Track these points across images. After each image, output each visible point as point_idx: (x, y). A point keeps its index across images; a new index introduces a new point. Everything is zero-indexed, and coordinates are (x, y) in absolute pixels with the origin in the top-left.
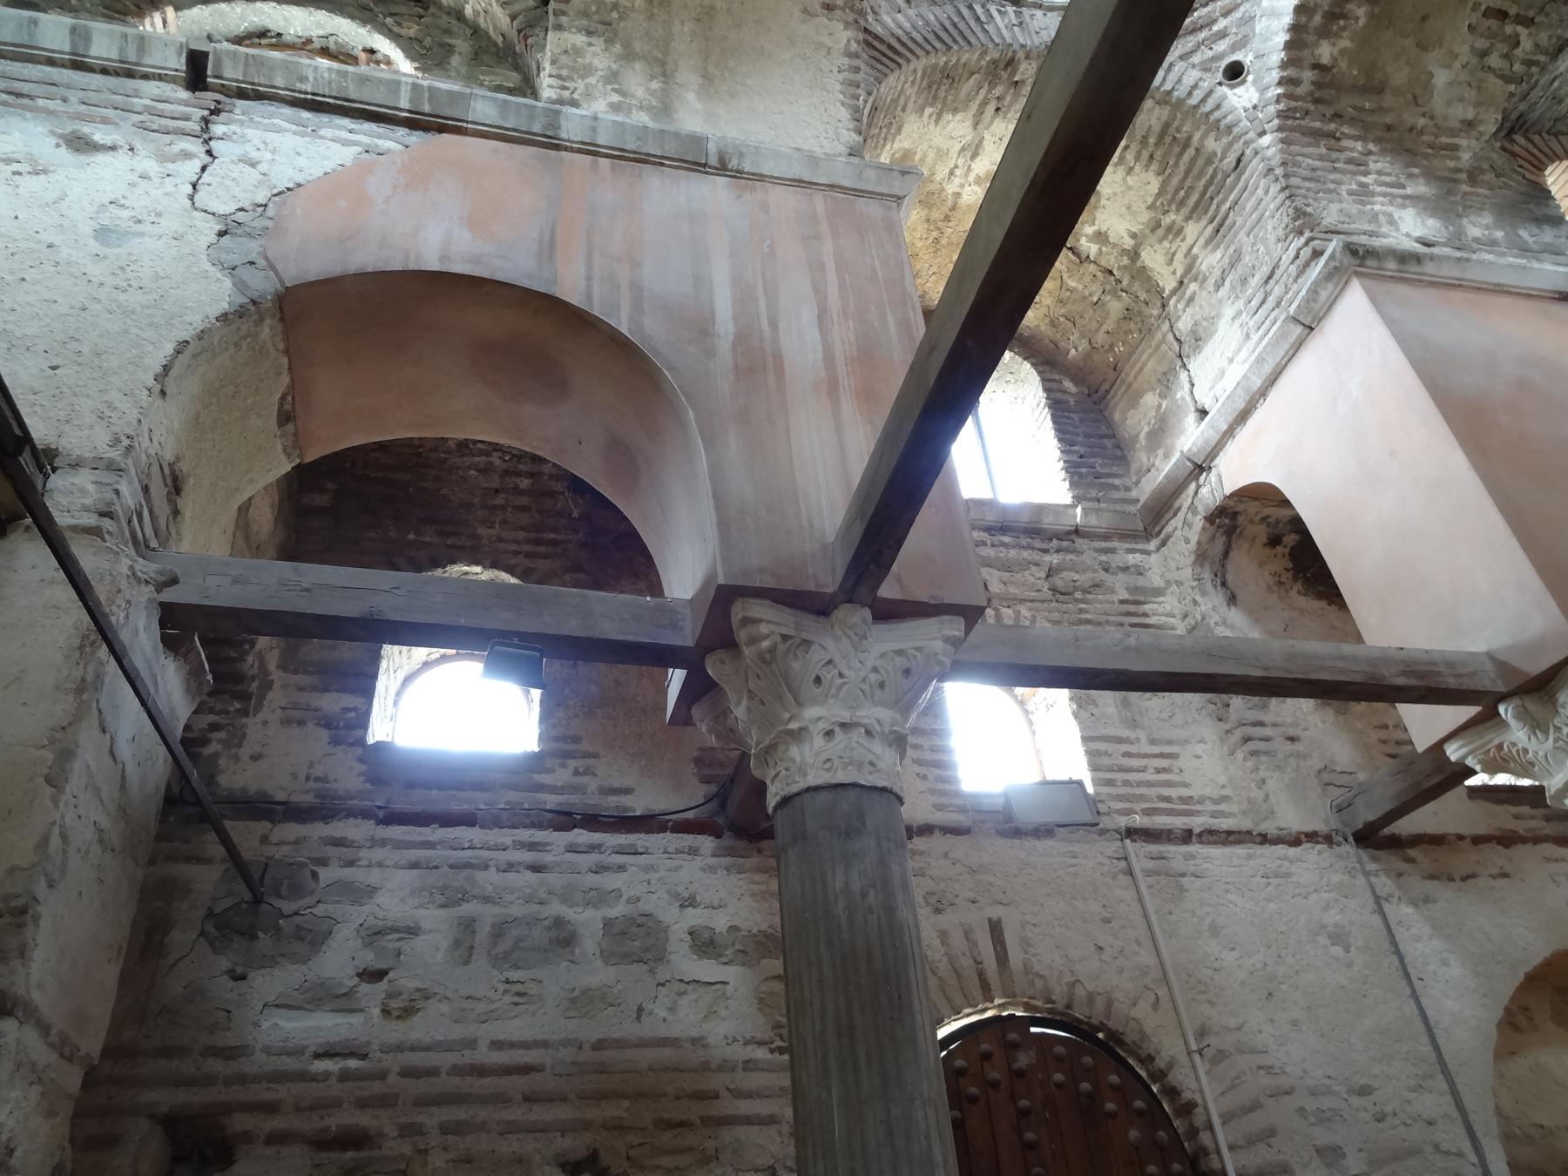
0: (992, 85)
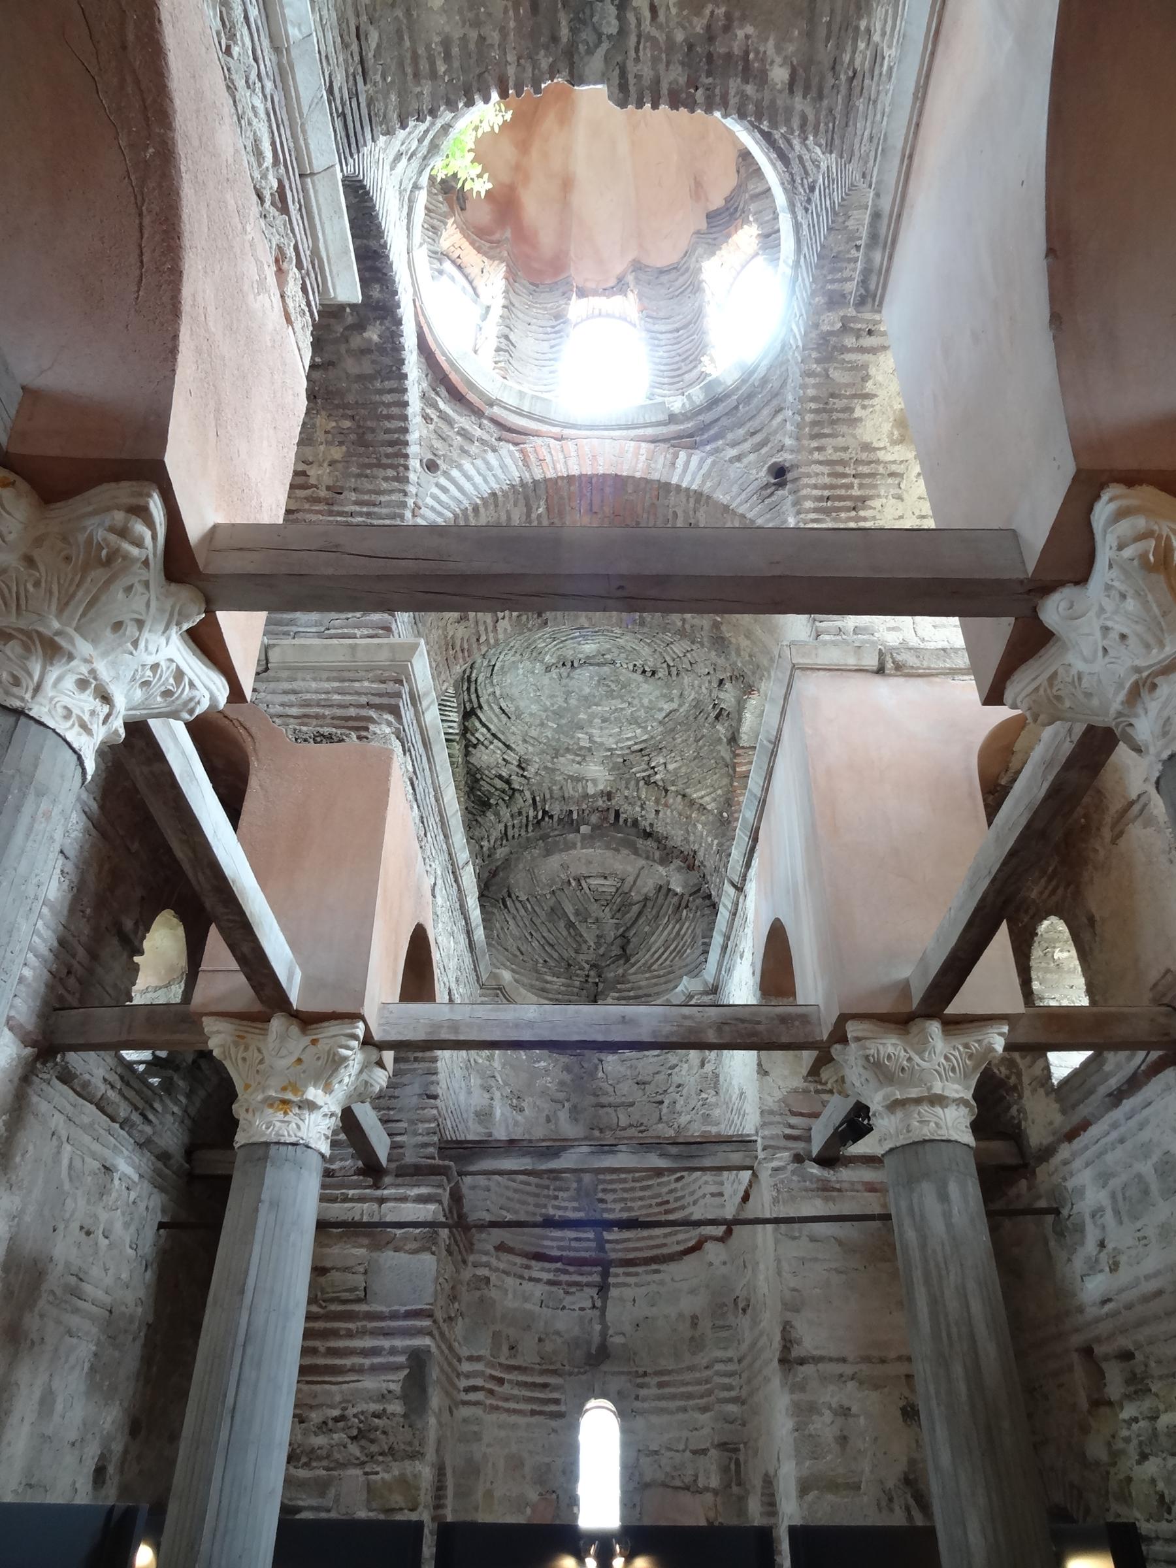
0: (844, 350)
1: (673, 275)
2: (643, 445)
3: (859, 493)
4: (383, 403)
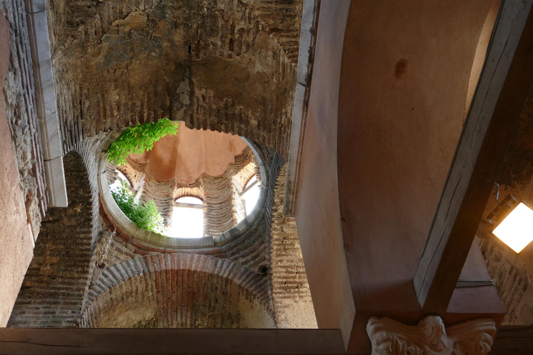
1: (220, 180)
2: (203, 256)
3: (299, 280)
4: (80, 238)
